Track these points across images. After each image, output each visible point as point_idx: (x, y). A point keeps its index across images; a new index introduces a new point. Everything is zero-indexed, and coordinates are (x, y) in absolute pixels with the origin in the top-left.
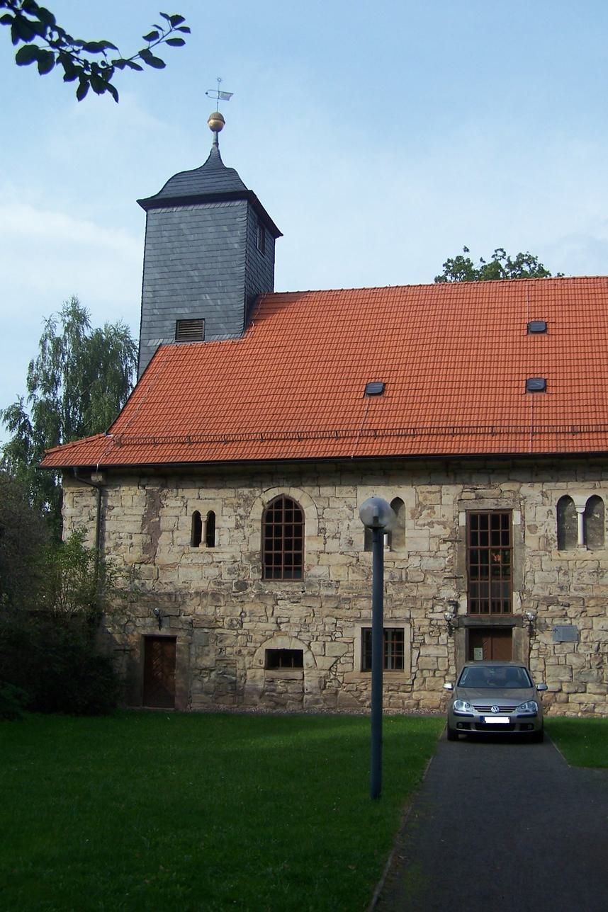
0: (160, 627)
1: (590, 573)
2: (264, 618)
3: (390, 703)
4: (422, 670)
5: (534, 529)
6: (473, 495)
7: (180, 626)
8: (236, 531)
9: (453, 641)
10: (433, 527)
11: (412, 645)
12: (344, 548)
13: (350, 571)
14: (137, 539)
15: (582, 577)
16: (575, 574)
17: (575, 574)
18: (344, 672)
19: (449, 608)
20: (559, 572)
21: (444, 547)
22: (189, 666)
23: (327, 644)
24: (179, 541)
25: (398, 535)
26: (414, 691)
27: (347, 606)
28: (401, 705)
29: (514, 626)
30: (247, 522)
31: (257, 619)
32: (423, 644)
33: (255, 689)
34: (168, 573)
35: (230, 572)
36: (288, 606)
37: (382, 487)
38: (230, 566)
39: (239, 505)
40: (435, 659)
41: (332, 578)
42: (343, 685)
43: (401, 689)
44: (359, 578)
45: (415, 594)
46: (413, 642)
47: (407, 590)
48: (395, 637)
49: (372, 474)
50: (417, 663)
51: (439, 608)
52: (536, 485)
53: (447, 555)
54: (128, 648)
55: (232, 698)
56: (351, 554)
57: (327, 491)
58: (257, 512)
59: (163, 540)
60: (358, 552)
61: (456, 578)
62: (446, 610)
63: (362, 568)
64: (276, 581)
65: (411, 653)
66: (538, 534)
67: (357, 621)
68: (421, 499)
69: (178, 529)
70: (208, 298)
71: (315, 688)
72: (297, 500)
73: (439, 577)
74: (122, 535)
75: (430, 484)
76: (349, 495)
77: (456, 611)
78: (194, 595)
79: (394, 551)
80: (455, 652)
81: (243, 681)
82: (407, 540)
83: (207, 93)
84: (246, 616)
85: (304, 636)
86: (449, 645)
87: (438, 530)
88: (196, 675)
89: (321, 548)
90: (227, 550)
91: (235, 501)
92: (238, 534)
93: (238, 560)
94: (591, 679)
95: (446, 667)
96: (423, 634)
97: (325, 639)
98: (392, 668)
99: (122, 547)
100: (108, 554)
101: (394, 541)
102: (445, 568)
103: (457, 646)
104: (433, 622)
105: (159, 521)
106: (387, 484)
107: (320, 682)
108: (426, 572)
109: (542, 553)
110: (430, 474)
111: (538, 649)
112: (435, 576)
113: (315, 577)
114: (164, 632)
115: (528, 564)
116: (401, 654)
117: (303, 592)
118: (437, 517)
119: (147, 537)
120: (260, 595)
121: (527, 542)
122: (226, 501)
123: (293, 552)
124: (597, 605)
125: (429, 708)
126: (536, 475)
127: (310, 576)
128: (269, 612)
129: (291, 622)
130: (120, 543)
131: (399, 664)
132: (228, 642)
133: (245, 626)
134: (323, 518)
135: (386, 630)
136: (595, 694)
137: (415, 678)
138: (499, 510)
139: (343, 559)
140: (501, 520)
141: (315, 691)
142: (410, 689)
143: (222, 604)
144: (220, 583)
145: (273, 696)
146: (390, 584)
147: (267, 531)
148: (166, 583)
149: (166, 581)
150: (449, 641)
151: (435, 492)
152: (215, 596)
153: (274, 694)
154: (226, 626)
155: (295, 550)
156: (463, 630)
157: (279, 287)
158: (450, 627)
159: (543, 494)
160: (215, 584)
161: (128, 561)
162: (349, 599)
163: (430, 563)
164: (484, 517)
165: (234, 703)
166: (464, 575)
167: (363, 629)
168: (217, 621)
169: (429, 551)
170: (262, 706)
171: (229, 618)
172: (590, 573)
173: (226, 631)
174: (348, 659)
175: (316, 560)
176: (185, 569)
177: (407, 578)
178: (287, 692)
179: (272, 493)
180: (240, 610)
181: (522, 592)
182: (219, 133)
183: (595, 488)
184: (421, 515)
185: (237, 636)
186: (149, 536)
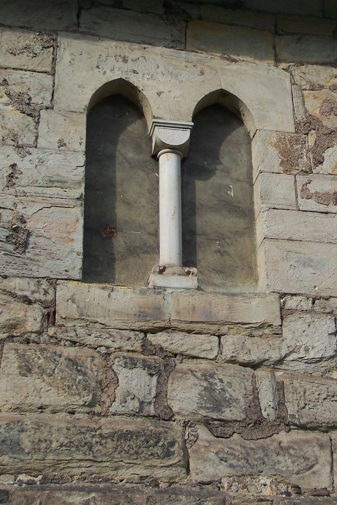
25: (221, 237)
37: (159, 50)
44: (53, 397)
47: (285, 463)
60: (53, 282)
63: (71, 352)
106: (179, 43)
146: (203, 433)
177: (281, 404)
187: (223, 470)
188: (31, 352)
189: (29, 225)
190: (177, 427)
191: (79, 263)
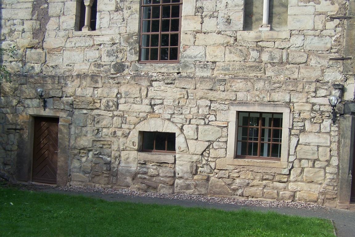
0: (45, 107)
2: (138, 99)
3: (263, 193)
4: (300, 160)
7: (62, 107)
8: (115, 13)
9: (337, 129)
11: (290, 131)
12: (222, 27)
13: (227, 51)
14: (28, 25)
18: (217, 158)
19: (334, 92)
21: (331, 25)
22: (69, 146)
23: (200, 127)
24: (64, 26)
26: (290, 182)
27: (222, 88)
28: (276, 196)
31: (131, 100)
33: (128, 171)
34: (54, 57)
35: (109, 54)
36: (162, 88)
38: (109, 48)
40: (316, 148)
41: (209, 59)
42: (216, 171)
43: (277, 178)
44: (236, 59)
45: (295, 76)
46: (292, 129)
47: (287, 72)
48: (272, 122)
51: (322, 92)
53: (333, 33)
54: (18, 127)
55: (106, 179)
56: (229, 33)
59: (51, 25)
60: (236, 32)
61: (343, 59)
62: (330, 94)
63: (240, 48)
65: (290, 140)
67: (232, 104)
69: (63, 14)
71: (187, 172)
73: (324, 58)
74: (15, 22)
77: (342, 96)
78: (75, 78)
79: (274, 30)
80: (339, 142)
81: (117, 163)
82: (289, 19)
84: (121, 97)
85: (178, 119)
86: (332, 133)
88: (75, 155)
89: (198, 27)
90: (107, 33)
92: (117, 16)
93: (117, 41)
95: (328, 158)
96: (304, 120)
97: (198, 122)
98: (268, 155)
99: (16, 33)
100: (4, 40)
101: (275, 20)
102: (331, 48)
103: (341, 134)
104: (316, 108)
105: (48, 8)
107: (191, 167)
108: (309, 53)
112: (319, 57)
113: (191, 57)
114: (47, 113)
116: (277, 141)
117: (178, 73)
119: (36, 23)
120: (137, 77)
125: (306, 201)
127: (186, 57)
128: (144, 94)
129: (165, 103)
130: (13, 29)
131: (275, 151)
132: (104, 123)
133: (121, 107)
135: (264, 116)
137: (293, 167)
139: (220, 39)
141: (186, 176)
142: (285, 180)
143: (100, 85)
144: (99, 66)
145: (145, 178)
146: (269, 65)
148: (52, 67)
149: (53, 65)
150: (332, 129)
152: (94, 78)
153: (146, 176)
154: (103, 107)
156: (349, 117)
158: (334, 113)
160: (95, 67)
161: (20, 45)
163: (314, 43)
165: (108, 184)
167: (238, 113)
168: (95, 103)
169: (314, 29)
170: (134, 189)
171: (106, 99)
173: (102, 112)
174: (221, 144)
175: (192, 40)
176: (69, 52)
177: (287, 58)
178: (158, 175)
180: (116, 91)
185: (113, 117)
186: (38, 22)
187: (272, 74)
188: (232, 48)
189: (231, 18)
190: (263, 64)
191: (242, 26)
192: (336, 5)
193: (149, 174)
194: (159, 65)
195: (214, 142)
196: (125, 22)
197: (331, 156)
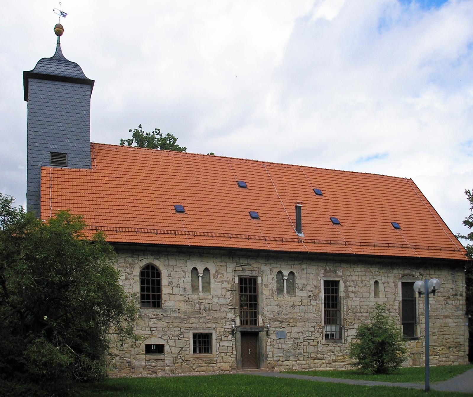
1: (290, 307)
4: (221, 353)
5: (267, 286)
6: (241, 269)
9: (234, 339)
10: (223, 283)
12: (181, 292)
13: (185, 304)
15: (287, 309)
16: (284, 308)
17: (284, 308)
20: (277, 306)
29: (260, 331)
30: (132, 276)
32: (221, 340)
36: (156, 322)
39: (127, 268)
49: (194, 255)
50: (219, 350)
51: (228, 323)
52: (268, 265)
53: (230, 297)
55: (129, 370)
56: (186, 295)
57: (172, 262)
58: (137, 272)
61: (234, 308)
64: (149, 309)
66: (269, 288)
68: (217, 269)
70: (69, 142)
72: (158, 266)
73: (227, 308)
75: (221, 262)
76: (183, 265)
80: (236, 344)
83: (54, 10)
87: (225, 285)
91: (125, 265)
94: (291, 354)
95: (232, 352)
96: (221, 335)
108: (221, 305)
109: (270, 297)
110: (221, 257)
111: (270, 342)
115: (265, 302)
118: (225, 278)
121: (264, 292)
122: (120, 265)
123: (146, 293)
124: (293, 322)
126: (268, 260)
127: (165, 307)
134: (171, 276)
136: (292, 361)
138: (252, 276)
139: (182, 298)
140: (253, 280)
141: (171, 365)
147: (142, 282)
151: (224, 266)
153: (151, 367)
155: (157, 292)
157: (95, 138)
159: (271, 270)
162: (186, 318)
163: (222, 301)
164: (245, 279)
166: (238, 307)
172: (290, 307)
177: (212, 308)
178: (157, 366)
179: (144, 262)
181: (263, 315)
182: (60, 37)
183: (291, 268)
184: (217, 277)
192: (230, 284)
193: (152, 366)
194: (152, 310)
195: (183, 347)
196: (132, 286)
197: (233, 350)
